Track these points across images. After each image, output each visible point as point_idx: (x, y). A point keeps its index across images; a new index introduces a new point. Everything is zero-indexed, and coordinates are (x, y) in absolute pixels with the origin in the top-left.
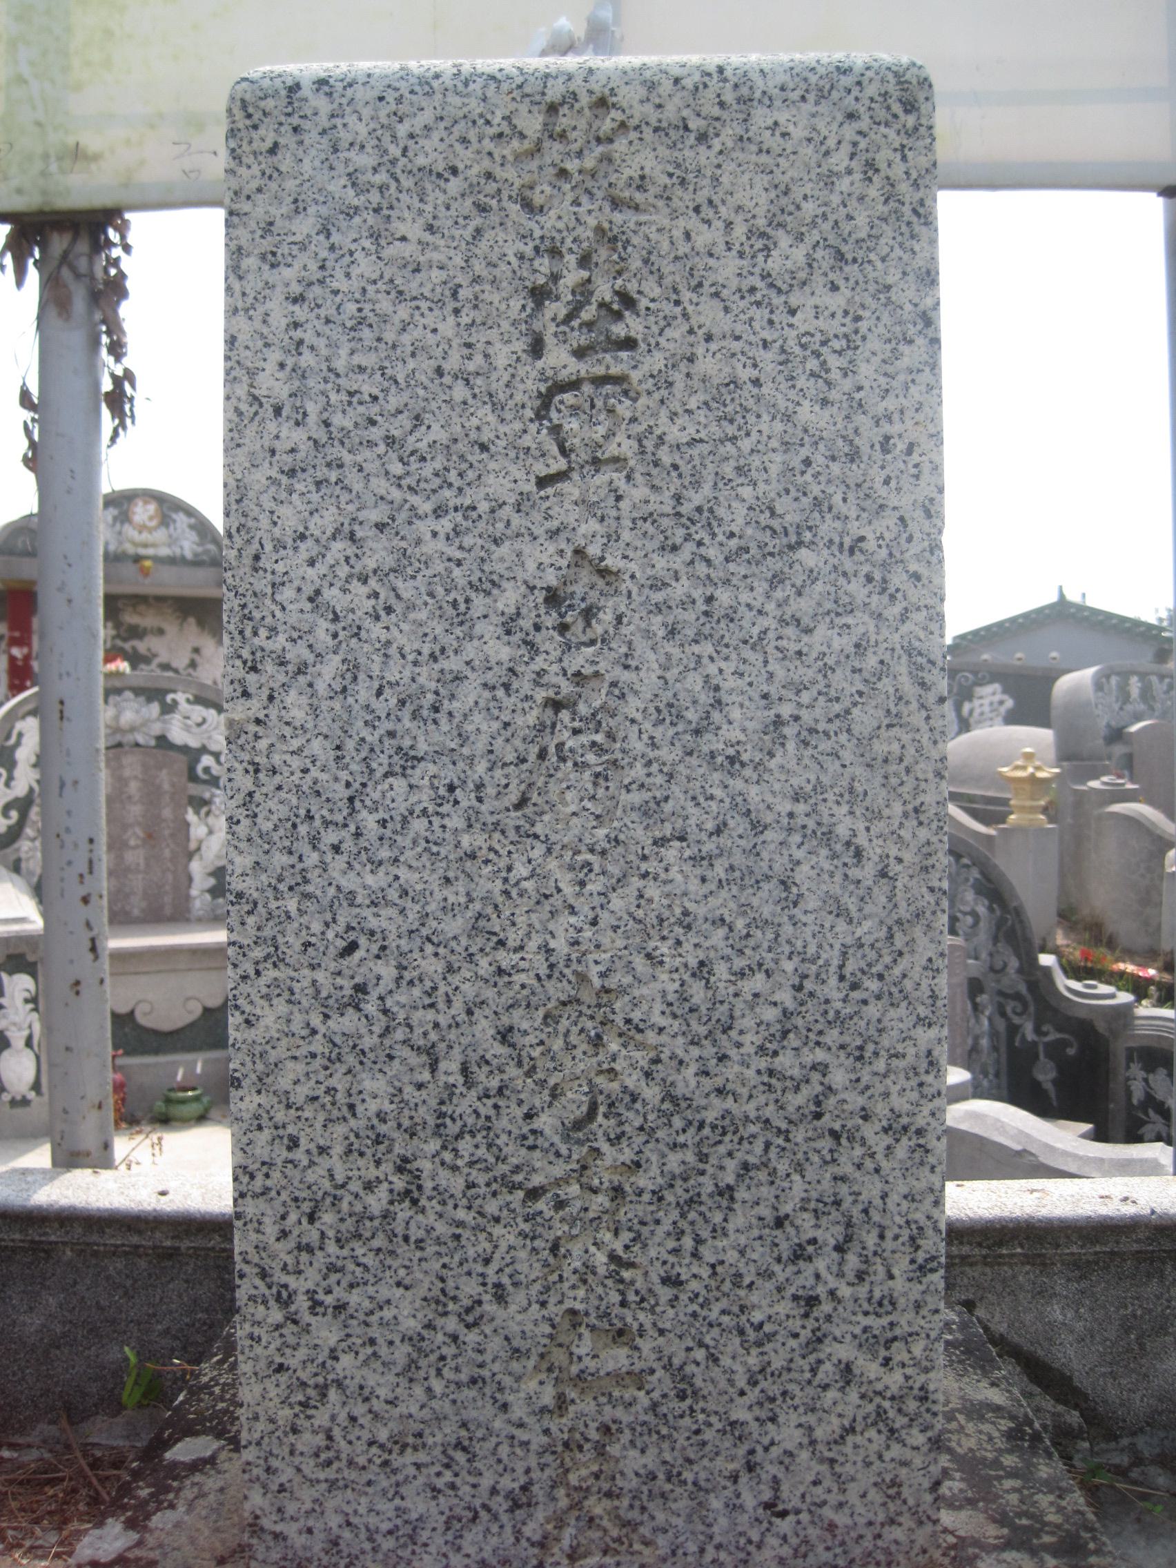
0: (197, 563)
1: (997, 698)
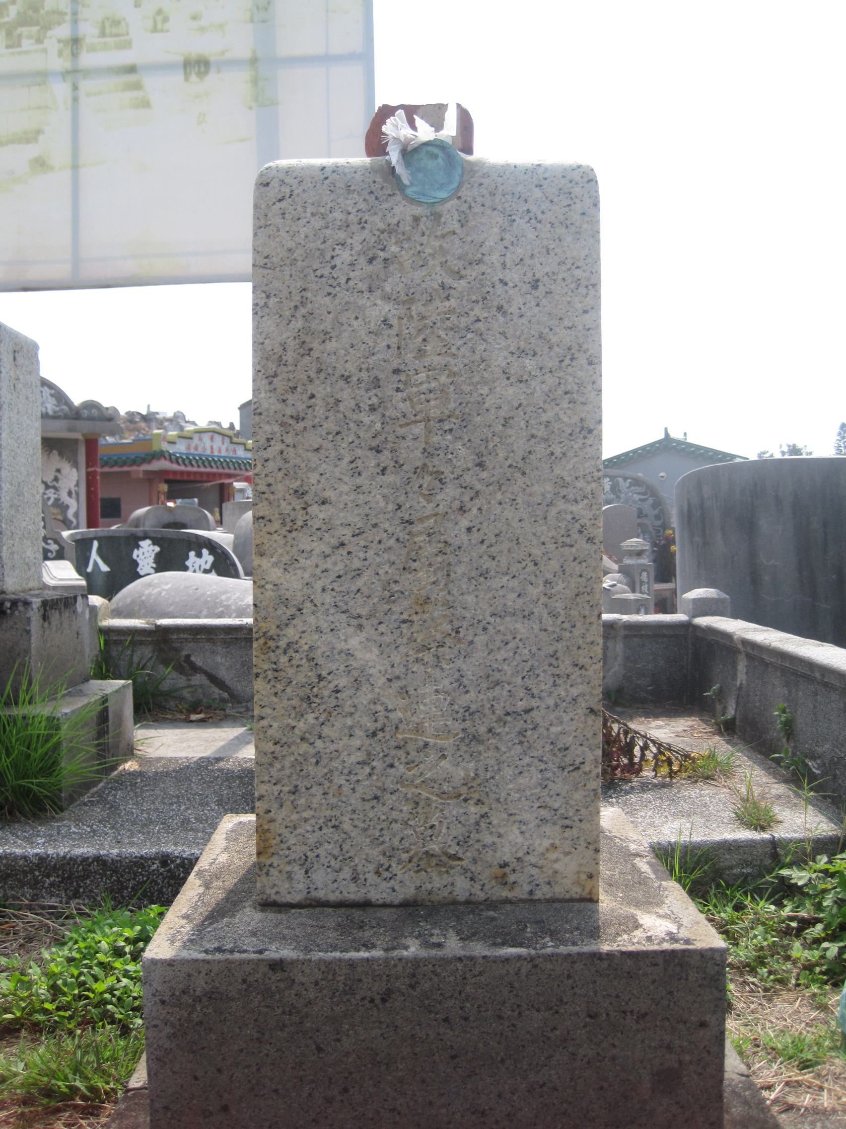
0: (55, 417)
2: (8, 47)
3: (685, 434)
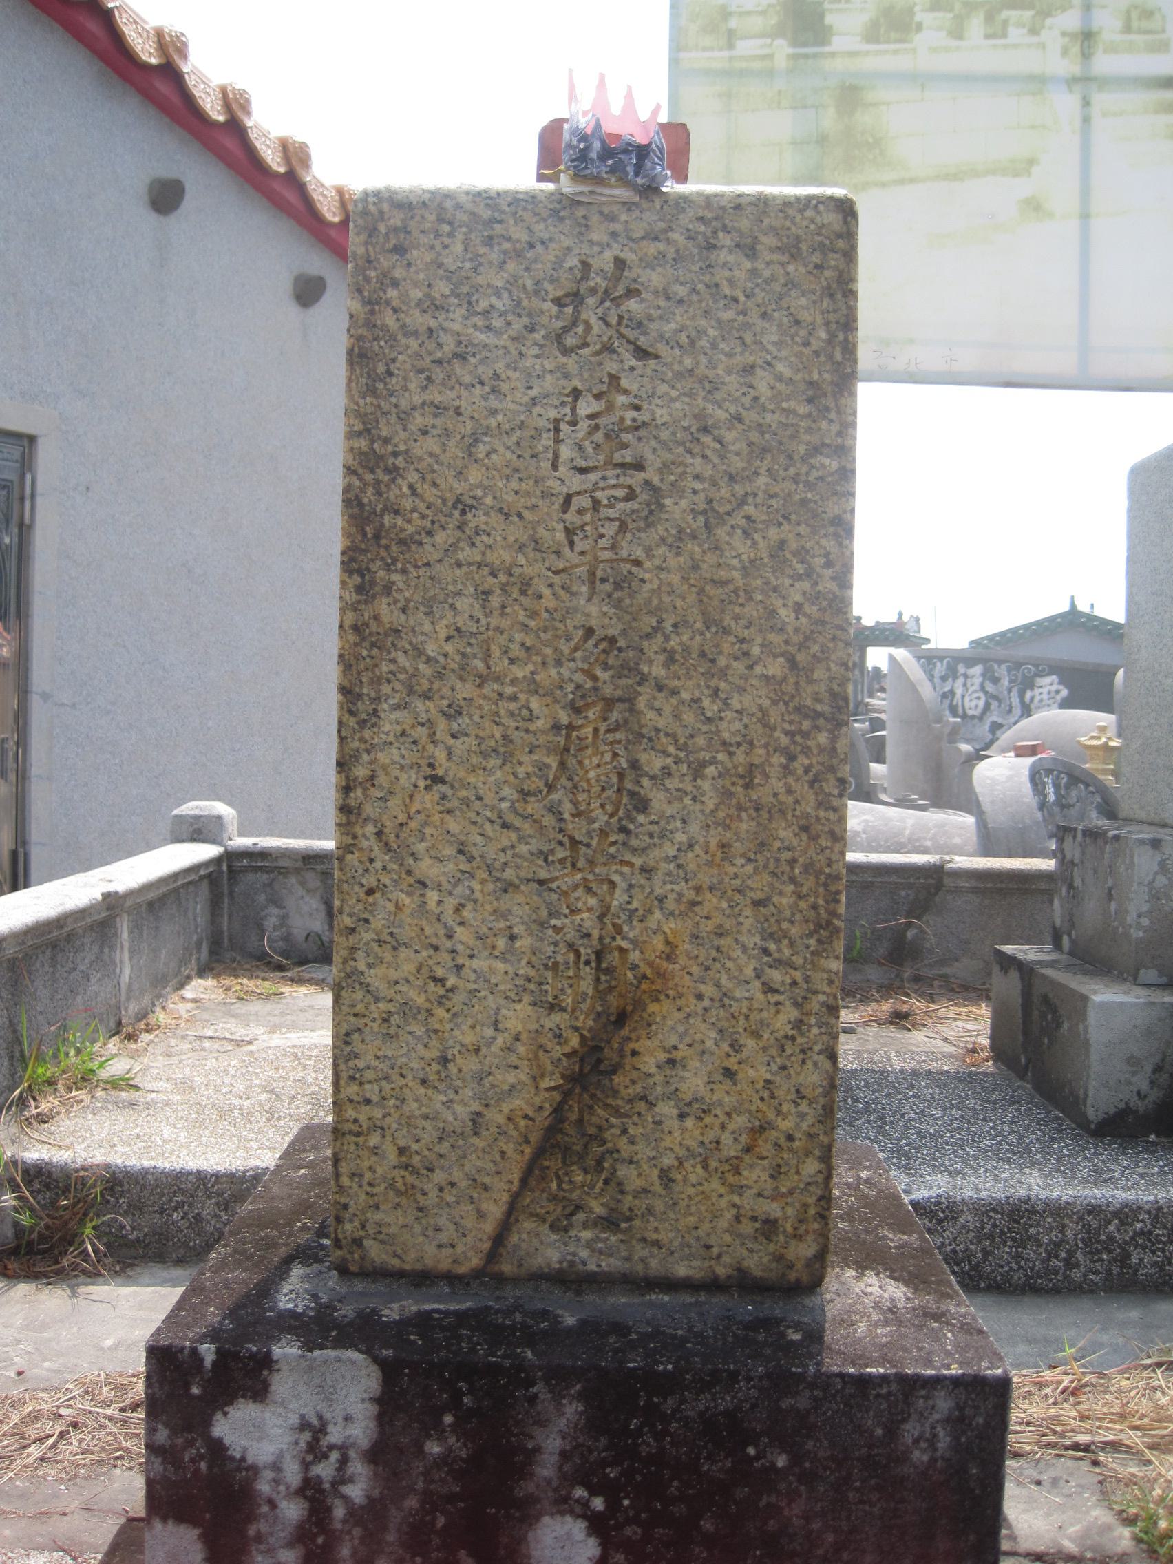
1: (1054, 688)
2: (987, 37)
3: (1092, 606)
